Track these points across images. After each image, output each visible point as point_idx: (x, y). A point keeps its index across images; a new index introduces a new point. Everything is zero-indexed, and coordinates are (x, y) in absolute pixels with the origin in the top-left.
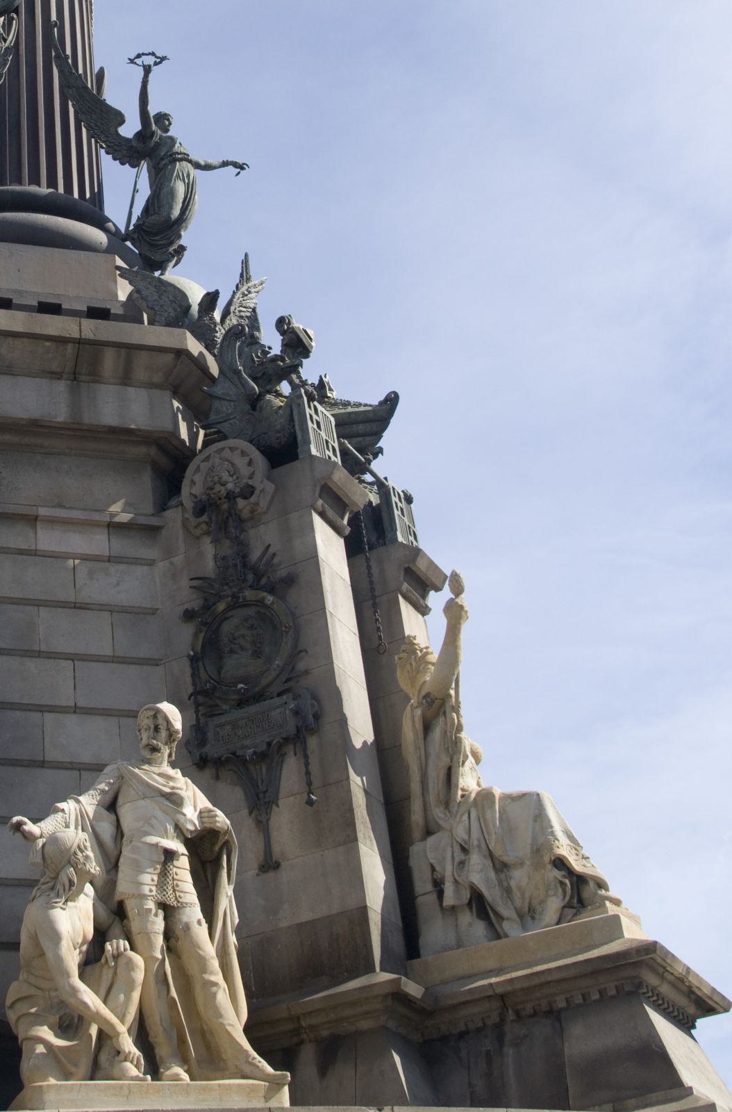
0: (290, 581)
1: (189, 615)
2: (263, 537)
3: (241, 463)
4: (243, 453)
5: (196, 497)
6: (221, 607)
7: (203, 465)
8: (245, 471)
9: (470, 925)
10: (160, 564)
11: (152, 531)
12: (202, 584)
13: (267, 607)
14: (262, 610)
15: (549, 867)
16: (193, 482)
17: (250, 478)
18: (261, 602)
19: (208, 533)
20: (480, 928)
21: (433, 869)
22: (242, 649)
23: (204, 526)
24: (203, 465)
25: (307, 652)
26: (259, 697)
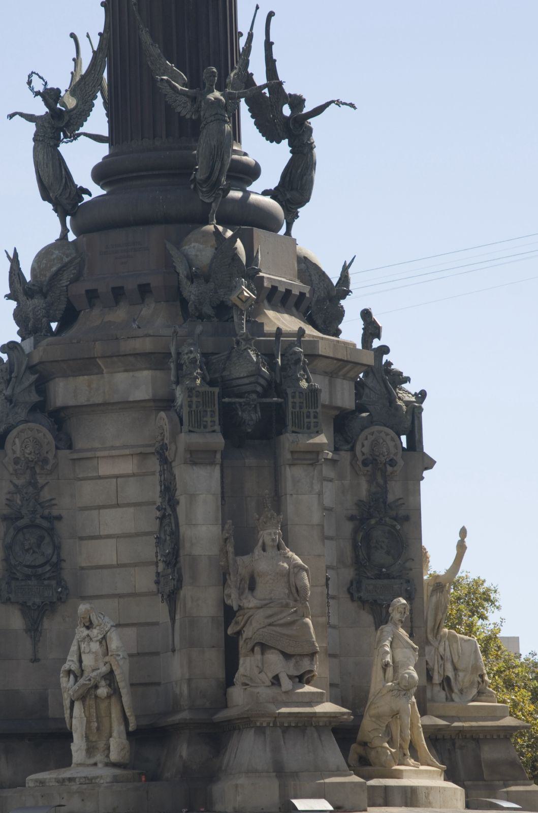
1: (351, 518)
2: (395, 491)
5: (363, 454)
6: (373, 522)
9: (439, 691)
10: (336, 481)
12: (359, 504)
13: (396, 530)
14: (392, 530)
15: (478, 676)
16: (363, 446)
17: (396, 454)
18: (394, 527)
19: (364, 475)
20: (442, 695)
21: (427, 663)
22: (381, 547)
25: (413, 560)
26: (388, 576)
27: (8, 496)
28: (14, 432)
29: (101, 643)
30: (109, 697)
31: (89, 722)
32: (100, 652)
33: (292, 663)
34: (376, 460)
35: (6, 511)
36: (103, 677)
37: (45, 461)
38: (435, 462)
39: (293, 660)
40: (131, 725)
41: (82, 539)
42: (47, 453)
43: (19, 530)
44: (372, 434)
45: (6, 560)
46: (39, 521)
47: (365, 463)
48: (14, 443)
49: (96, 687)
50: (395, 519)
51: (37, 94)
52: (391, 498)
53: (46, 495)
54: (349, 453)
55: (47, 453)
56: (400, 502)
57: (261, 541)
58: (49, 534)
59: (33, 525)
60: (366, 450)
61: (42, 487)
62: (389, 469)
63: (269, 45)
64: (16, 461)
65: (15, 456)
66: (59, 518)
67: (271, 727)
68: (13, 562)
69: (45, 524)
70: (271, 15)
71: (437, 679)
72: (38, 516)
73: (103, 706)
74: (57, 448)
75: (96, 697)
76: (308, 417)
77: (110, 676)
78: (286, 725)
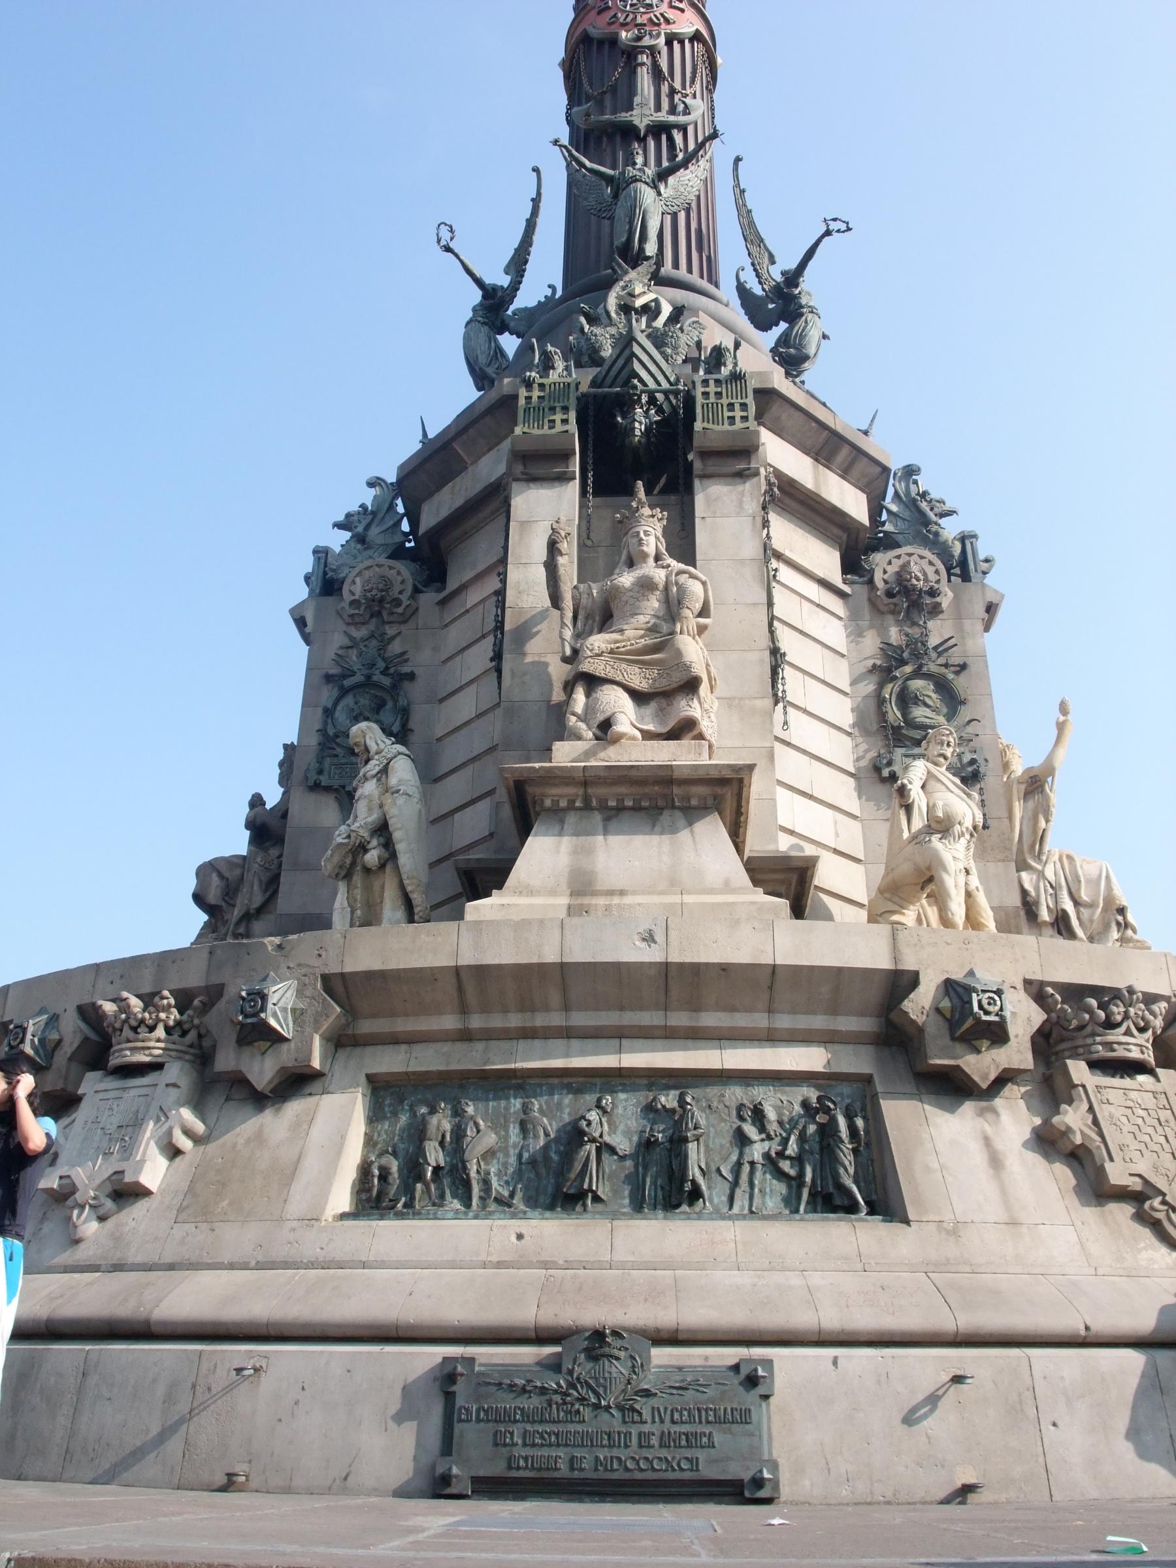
0: (963, 667)
3: (930, 571)
4: (931, 563)
6: (908, 669)
7: (894, 561)
8: (932, 577)
17: (938, 582)
23: (892, 607)
24: (894, 561)
27: (340, 652)
29: (378, 780)
30: (382, 866)
31: (352, 912)
32: (376, 793)
33: (650, 709)
34: (906, 587)
35: (335, 671)
36: (375, 831)
37: (398, 602)
38: (1003, 596)
39: (653, 705)
40: (416, 910)
41: (441, 701)
42: (400, 593)
43: (344, 692)
44: (899, 557)
45: (323, 731)
46: (377, 677)
47: (889, 594)
48: (354, 582)
49: (363, 848)
50: (946, 666)
51: (448, 249)
52: (933, 641)
53: (396, 648)
54: (866, 586)
55: (400, 593)
56: (950, 643)
57: (625, 553)
58: (392, 697)
59: (368, 683)
61: (393, 638)
62: (928, 600)
63: (740, 192)
65: (353, 598)
66: (411, 676)
67: (580, 809)
68: (331, 732)
69: (386, 681)
70: (738, 160)
71: (1045, 915)
72: (377, 672)
73: (377, 885)
74: (416, 591)
75: (367, 870)
76: (731, 407)
77: (382, 829)
78: (612, 803)
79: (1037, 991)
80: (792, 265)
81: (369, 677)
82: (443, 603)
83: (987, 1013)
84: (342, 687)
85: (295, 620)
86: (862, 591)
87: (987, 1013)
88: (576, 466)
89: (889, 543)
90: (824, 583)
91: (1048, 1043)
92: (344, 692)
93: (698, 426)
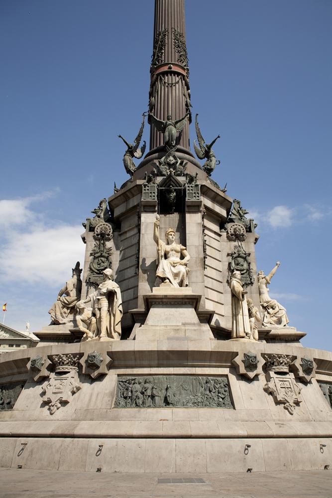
11: (220, 236)
28: (98, 225)
60: (232, 231)
64: (98, 235)
74: (113, 231)
79: (263, 355)
80: (209, 144)
81: (102, 254)
82: (120, 235)
83: (252, 362)
84: (95, 257)
85: (82, 238)
86: (224, 234)
87: (252, 362)
88: (156, 209)
89: (232, 221)
90: (215, 233)
91: (266, 368)
92: (95, 258)
93: (187, 198)
